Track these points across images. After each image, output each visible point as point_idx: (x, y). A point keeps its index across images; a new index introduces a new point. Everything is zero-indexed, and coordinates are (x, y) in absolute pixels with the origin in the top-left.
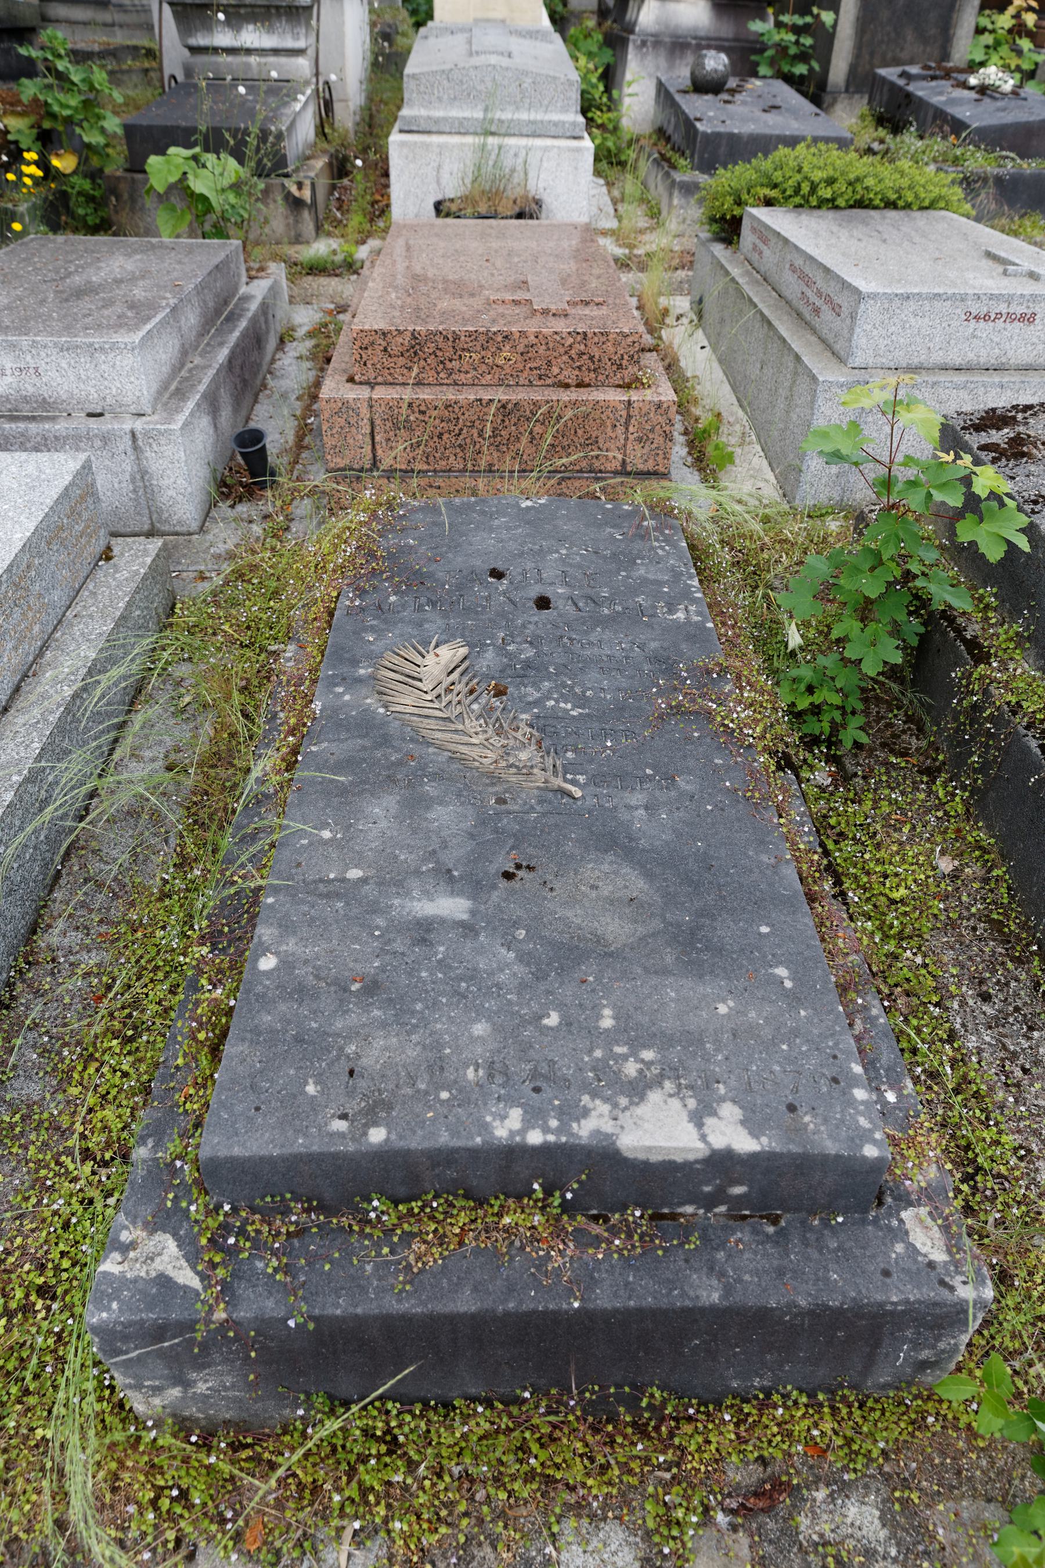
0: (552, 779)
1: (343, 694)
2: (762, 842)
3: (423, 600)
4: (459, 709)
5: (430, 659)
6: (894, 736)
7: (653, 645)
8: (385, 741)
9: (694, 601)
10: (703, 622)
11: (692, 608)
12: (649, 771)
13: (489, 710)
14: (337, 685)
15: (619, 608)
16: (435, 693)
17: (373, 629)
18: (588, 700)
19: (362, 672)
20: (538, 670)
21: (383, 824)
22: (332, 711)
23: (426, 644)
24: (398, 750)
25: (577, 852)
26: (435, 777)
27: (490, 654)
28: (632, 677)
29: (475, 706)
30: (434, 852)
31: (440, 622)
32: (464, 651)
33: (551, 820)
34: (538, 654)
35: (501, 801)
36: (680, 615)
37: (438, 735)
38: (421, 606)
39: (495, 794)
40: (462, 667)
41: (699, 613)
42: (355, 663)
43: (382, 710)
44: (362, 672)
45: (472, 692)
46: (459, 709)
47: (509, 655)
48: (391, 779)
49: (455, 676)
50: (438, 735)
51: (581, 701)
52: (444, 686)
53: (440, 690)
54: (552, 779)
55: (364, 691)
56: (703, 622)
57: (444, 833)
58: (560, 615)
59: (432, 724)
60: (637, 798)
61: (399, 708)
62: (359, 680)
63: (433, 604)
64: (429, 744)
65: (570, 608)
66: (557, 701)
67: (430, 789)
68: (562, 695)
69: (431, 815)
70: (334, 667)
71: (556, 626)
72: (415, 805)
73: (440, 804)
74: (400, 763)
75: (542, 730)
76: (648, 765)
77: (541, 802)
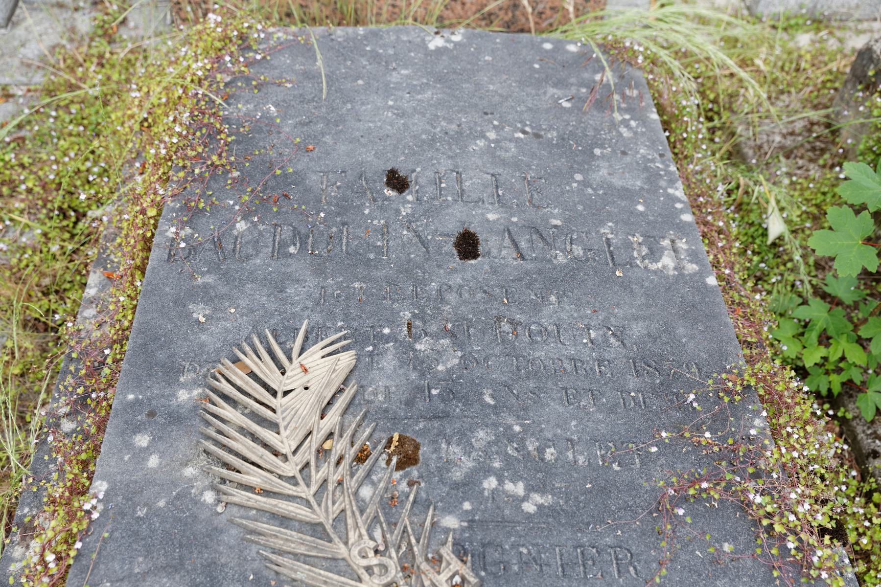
1: (147, 451)
3: (286, 232)
5: (294, 378)
7: (637, 329)
9: (682, 229)
10: (702, 274)
11: (682, 245)
13: (390, 502)
14: (137, 429)
15: (578, 251)
16: (299, 459)
17: (205, 294)
19: (183, 395)
20: (466, 401)
27: (389, 361)
29: (366, 492)
31: (311, 282)
32: (346, 359)
34: (464, 364)
36: (667, 261)
38: (283, 245)
41: (694, 257)
42: (171, 373)
43: (209, 497)
44: (183, 395)
45: (361, 457)
46: (344, 502)
47: (422, 365)
49: (333, 417)
51: (540, 475)
53: (308, 453)
55: (183, 445)
56: (702, 274)
58: (494, 271)
59: (293, 540)
62: (176, 418)
63: (299, 238)
65: (508, 253)
66: (501, 481)
70: (138, 383)
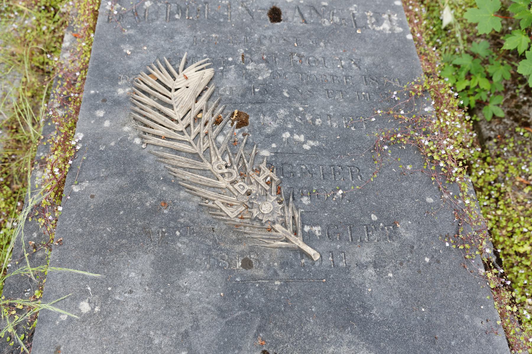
0: (292, 238)
1: (103, 119)
2: (474, 302)
3: (173, 7)
4: (208, 143)
5: (180, 82)
6: (517, 106)
7: (367, 61)
8: (140, 182)
9: (395, 9)
10: (404, 33)
11: (395, 17)
12: (374, 217)
13: (233, 144)
14: (97, 108)
15: (337, 19)
16: (185, 122)
17: (130, 40)
18: (317, 129)
19: (121, 91)
20: (274, 95)
21: (139, 294)
22: (93, 140)
23: (175, 59)
24: (153, 194)
25: (318, 331)
26: (187, 229)
27: (232, 75)
28: (352, 101)
29: (221, 139)
30: (186, 334)
31: (188, 34)
32: (209, 73)
33: (292, 291)
34: (273, 76)
35: (247, 264)
36: (386, 26)
37: (188, 176)
38: (172, 14)
39: (241, 253)
40: (210, 91)
41: (401, 24)
42: (114, 80)
43: (138, 141)
44: (121, 91)
45: (217, 122)
46: (208, 143)
47: (249, 76)
48: (146, 232)
49: (202, 102)
50: (188, 176)
51: (312, 132)
52: (192, 114)
53: (189, 119)
54: (292, 238)
55: (123, 116)
56: (404, 33)
57: (196, 308)
58: (290, 29)
59: (182, 161)
60: (366, 254)
61: (154, 140)
62: (117, 102)
63: (182, 10)
64: (181, 188)
65: (298, 20)
66: (292, 134)
67: (182, 246)
68: (296, 124)
69: (183, 283)
70: (96, 85)
71: (288, 42)
72: (169, 267)
73: (191, 267)
74: (155, 211)
75: (280, 171)
76: (373, 210)
77: (283, 265)
